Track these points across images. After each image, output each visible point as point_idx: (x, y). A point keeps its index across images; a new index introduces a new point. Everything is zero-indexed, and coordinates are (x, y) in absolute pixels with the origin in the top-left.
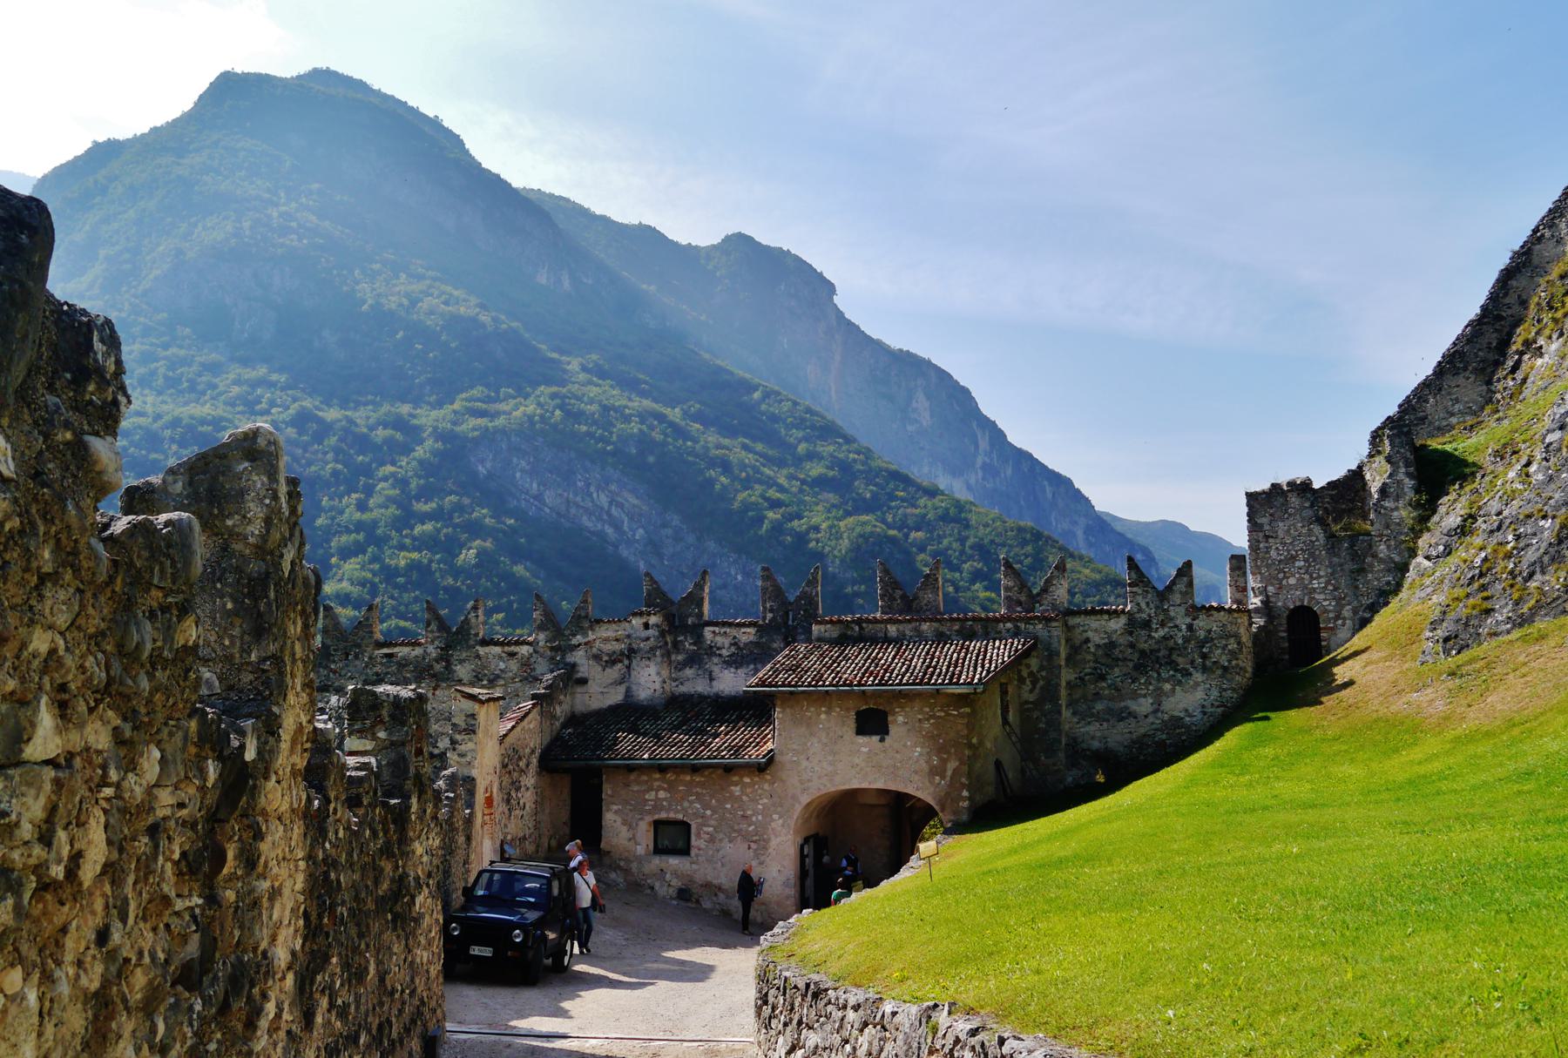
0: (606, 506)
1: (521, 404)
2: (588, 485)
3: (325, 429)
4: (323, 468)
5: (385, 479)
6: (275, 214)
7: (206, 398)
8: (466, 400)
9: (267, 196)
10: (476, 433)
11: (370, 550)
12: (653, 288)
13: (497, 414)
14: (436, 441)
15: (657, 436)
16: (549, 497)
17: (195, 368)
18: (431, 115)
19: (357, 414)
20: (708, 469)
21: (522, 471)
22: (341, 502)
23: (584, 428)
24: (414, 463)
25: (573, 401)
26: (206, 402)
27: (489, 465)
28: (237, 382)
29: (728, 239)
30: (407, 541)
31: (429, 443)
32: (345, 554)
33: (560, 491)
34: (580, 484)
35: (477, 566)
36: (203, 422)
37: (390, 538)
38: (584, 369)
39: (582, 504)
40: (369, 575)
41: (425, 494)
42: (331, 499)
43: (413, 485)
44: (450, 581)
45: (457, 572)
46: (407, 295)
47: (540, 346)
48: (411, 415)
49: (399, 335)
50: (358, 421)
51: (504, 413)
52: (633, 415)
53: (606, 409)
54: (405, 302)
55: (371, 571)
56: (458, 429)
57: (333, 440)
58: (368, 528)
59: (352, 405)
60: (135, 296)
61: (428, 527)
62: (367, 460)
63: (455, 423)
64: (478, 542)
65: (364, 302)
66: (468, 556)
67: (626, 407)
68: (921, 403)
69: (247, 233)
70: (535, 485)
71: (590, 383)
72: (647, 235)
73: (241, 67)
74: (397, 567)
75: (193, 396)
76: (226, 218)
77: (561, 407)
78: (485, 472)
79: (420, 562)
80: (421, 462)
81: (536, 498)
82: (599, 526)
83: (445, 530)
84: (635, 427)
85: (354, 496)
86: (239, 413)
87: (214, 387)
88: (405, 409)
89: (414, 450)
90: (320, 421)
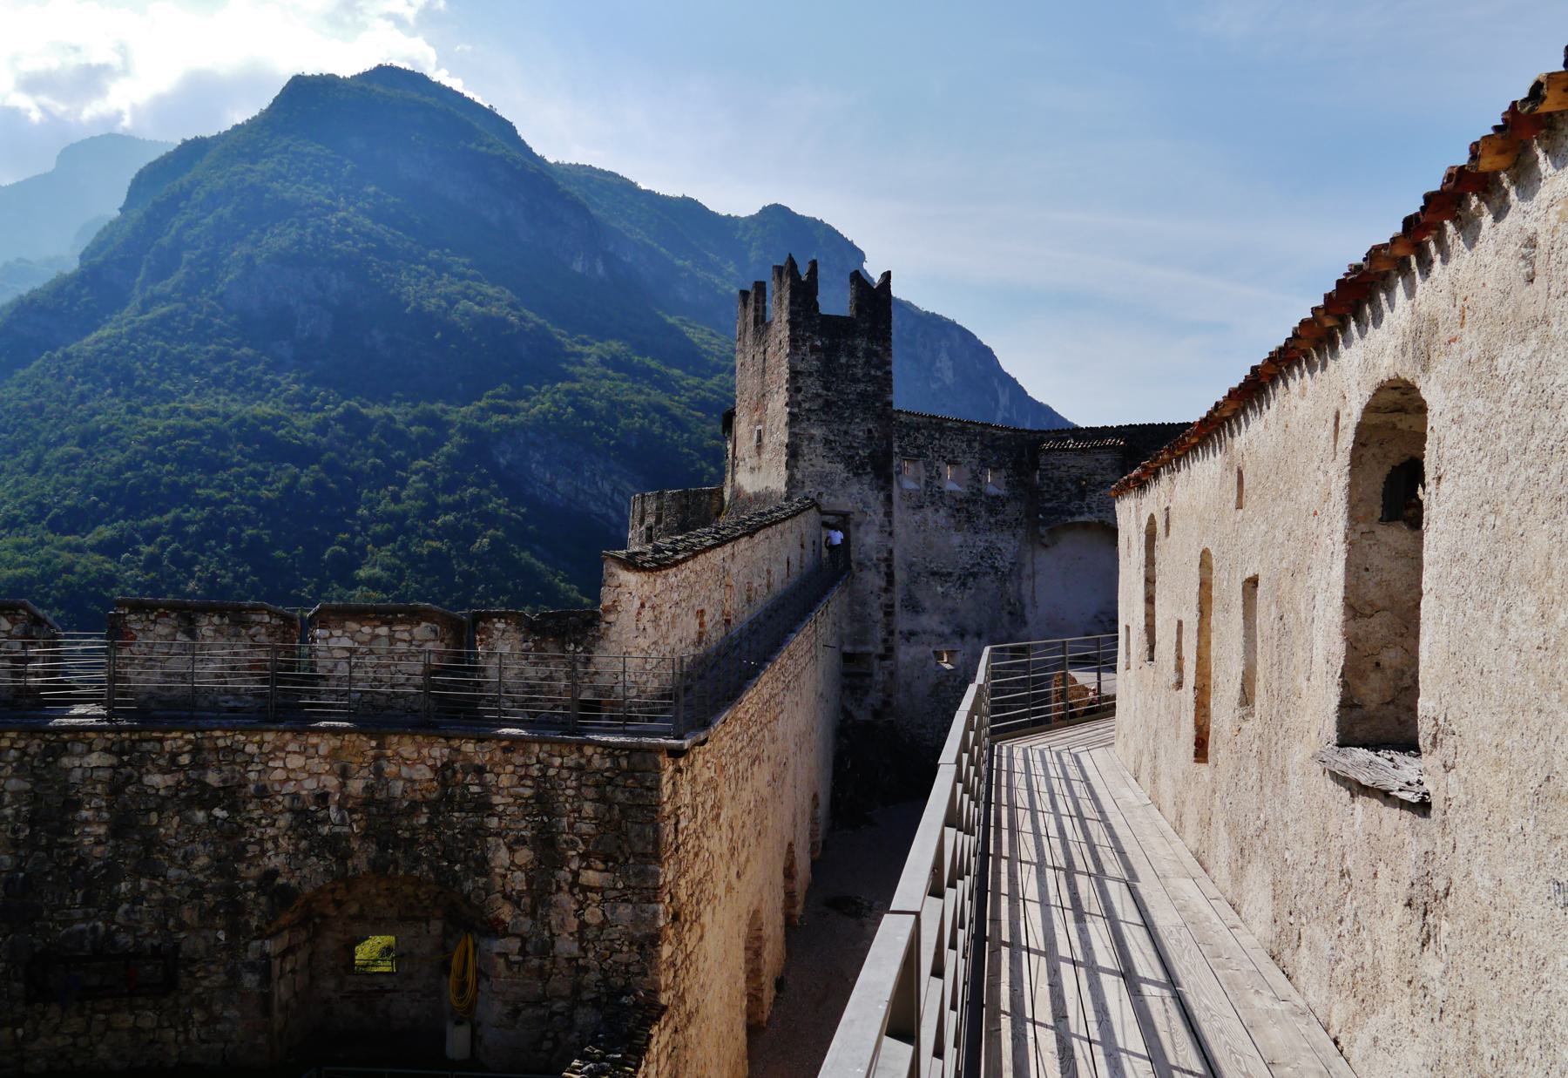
0: (609, 492)
1: (539, 400)
2: (595, 475)
3: (368, 423)
4: (365, 463)
5: (416, 472)
6: (334, 220)
7: (270, 395)
8: (493, 397)
9: (328, 201)
10: (498, 430)
11: (399, 539)
12: (688, 263)
13: (514, 412)
14: (463, 437)
15: (657, 429)
16: (560, 485)
17: (261, 367)
18: (486, 106)
19: (399, 410)
20: (700, 459)
21: (538, 462)
22: (378, 493)
23: (592, 423)
24: (442, 459)
25: (583, 399)
26: (269, 400)
27: (509, 456)
28: (296, 381)
29: (765, 210)
30: (430, 530)
31: (457, 439)
32: (379, 541)
33: (569, 480)
34: (587, 474)
35: (489, 552)
36: (264, 421)
37: (417, 527)
38: (603, 361)
39: (589, 491)
40: (398, 562)
41: (449, 488)
42: (371, 491)
43: (440, 479)
44: (466, 567)
45: (470, 558)
46: (446, 297)
47: (563, 339)
48: (444, 411)
49: (438, 335)
50: (397, 417)
51: (524, 410)
52: (635, 410)
53: (613, 404)
54: (444, 304)
55: (399, 558)
56: (483, 425)
57: (373, 438)
58: (398, 520)
59: (394, 401)
60: (212, 298)
61: (450, 518)
62: (403, 454)
63: (480, 420)
64: (490, 532)
65: (408, 304)
66: (483, 543)
67: (632, 402)
68: (945, 364)
69: (309, 239)
70: (548, 475)
71: (605, 377)
72: (689, 209)
73: (311, 68)
74: (421, 555)
75: (259, 393)
76: (292, 225)
77: (572, 404)
78: (505, 463)
79: (440, 549)
80: (449, 456)
81: (548, 486)
82: (604, 511)
83: (464, 521)
84: (637, 422)
85: (390, 488)
86: (296, 410)
87: (276, 384)
88: (438, 406)
89: (443, 445)
90: (364, 418)
